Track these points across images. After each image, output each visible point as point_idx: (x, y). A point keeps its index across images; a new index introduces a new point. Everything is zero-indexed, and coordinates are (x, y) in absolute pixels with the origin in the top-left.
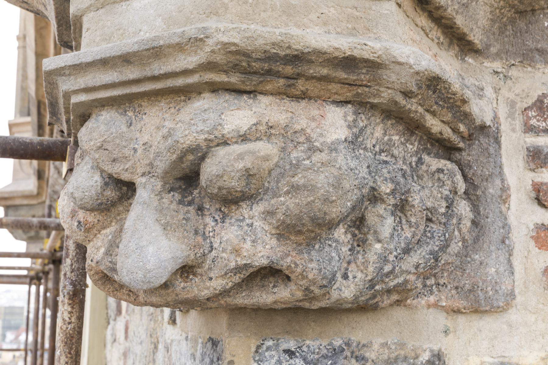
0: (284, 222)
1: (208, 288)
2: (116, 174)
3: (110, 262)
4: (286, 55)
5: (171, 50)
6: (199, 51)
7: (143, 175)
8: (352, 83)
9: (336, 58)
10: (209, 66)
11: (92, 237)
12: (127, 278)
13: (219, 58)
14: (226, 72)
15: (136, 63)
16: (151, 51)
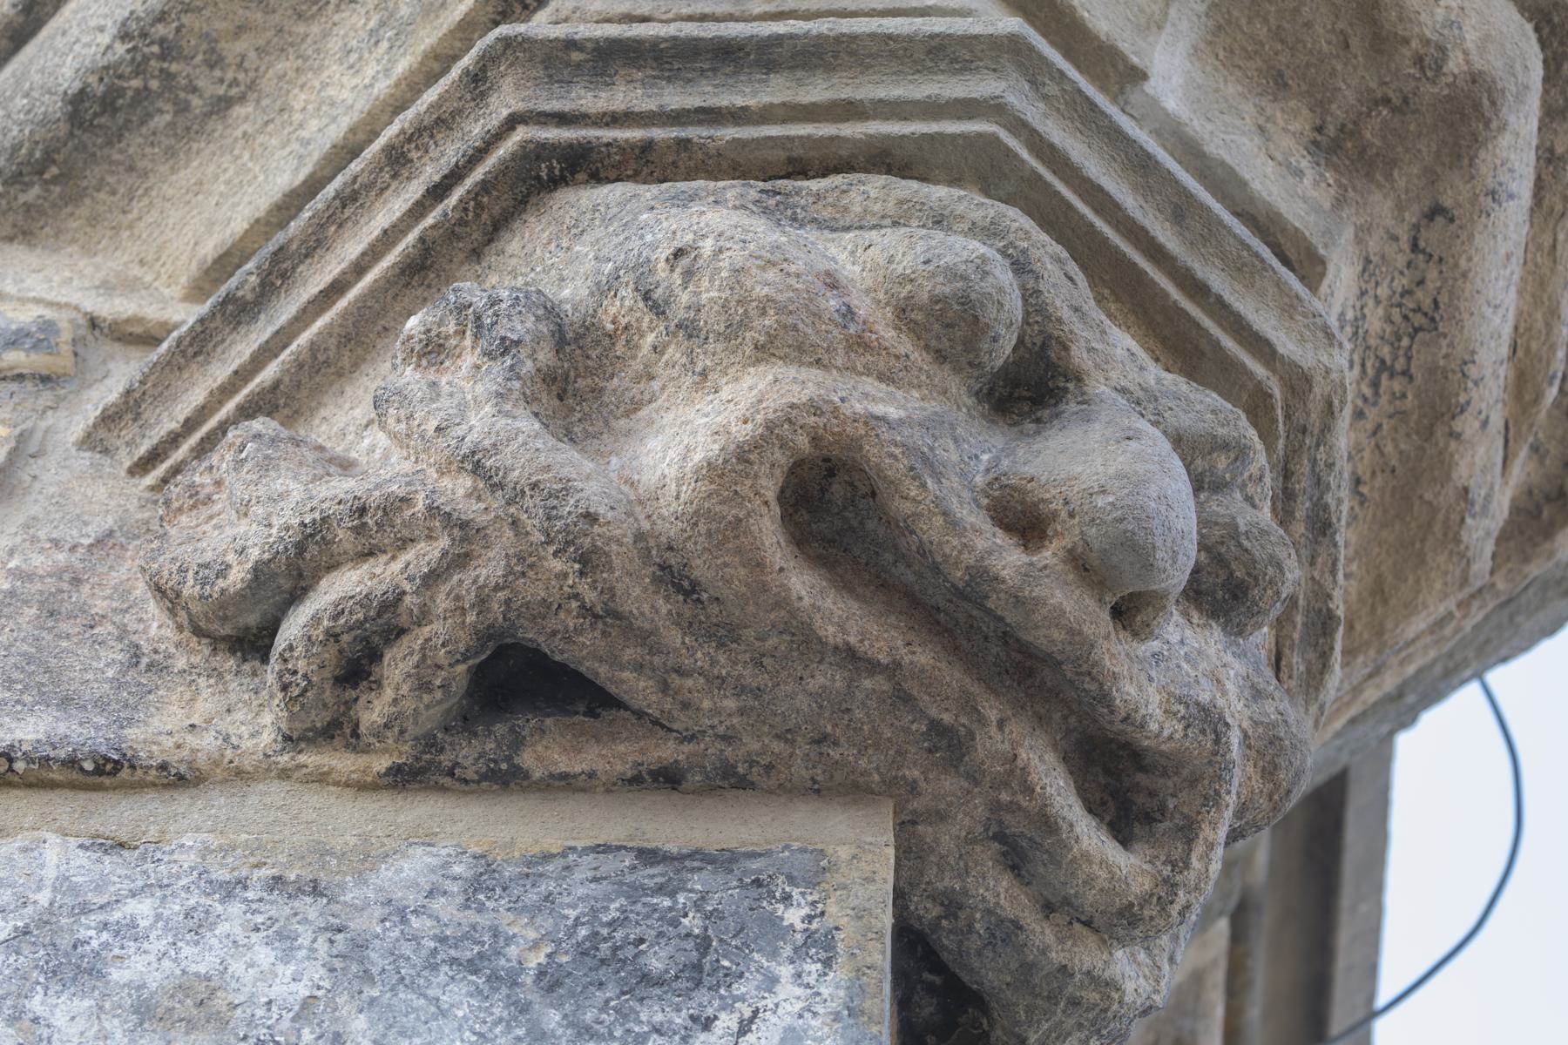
0: (1274, 725)
1: (1140, 688)
2: (1071, 332)
3: (932, 449)
4: (1326, 508)
5: (1272, 290)
6: (1309, 346)
7: (1123, 391)
8: (1283, 663)
9: (1329, 596)
10: (1298, 382)
11: (839, 362)
12: (1153, 505)
13: (1319, 389)
14: (1287, 417)
15: (1187, 234)
16: (1245, 254)
